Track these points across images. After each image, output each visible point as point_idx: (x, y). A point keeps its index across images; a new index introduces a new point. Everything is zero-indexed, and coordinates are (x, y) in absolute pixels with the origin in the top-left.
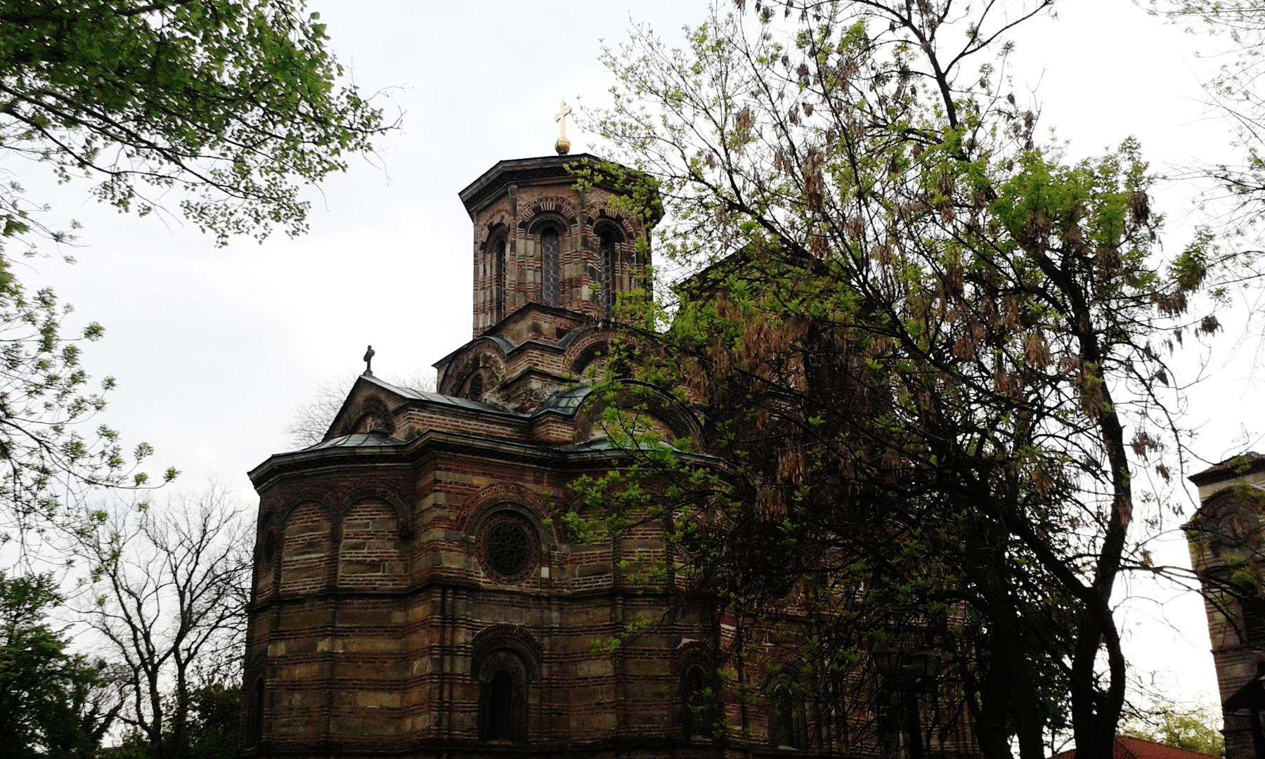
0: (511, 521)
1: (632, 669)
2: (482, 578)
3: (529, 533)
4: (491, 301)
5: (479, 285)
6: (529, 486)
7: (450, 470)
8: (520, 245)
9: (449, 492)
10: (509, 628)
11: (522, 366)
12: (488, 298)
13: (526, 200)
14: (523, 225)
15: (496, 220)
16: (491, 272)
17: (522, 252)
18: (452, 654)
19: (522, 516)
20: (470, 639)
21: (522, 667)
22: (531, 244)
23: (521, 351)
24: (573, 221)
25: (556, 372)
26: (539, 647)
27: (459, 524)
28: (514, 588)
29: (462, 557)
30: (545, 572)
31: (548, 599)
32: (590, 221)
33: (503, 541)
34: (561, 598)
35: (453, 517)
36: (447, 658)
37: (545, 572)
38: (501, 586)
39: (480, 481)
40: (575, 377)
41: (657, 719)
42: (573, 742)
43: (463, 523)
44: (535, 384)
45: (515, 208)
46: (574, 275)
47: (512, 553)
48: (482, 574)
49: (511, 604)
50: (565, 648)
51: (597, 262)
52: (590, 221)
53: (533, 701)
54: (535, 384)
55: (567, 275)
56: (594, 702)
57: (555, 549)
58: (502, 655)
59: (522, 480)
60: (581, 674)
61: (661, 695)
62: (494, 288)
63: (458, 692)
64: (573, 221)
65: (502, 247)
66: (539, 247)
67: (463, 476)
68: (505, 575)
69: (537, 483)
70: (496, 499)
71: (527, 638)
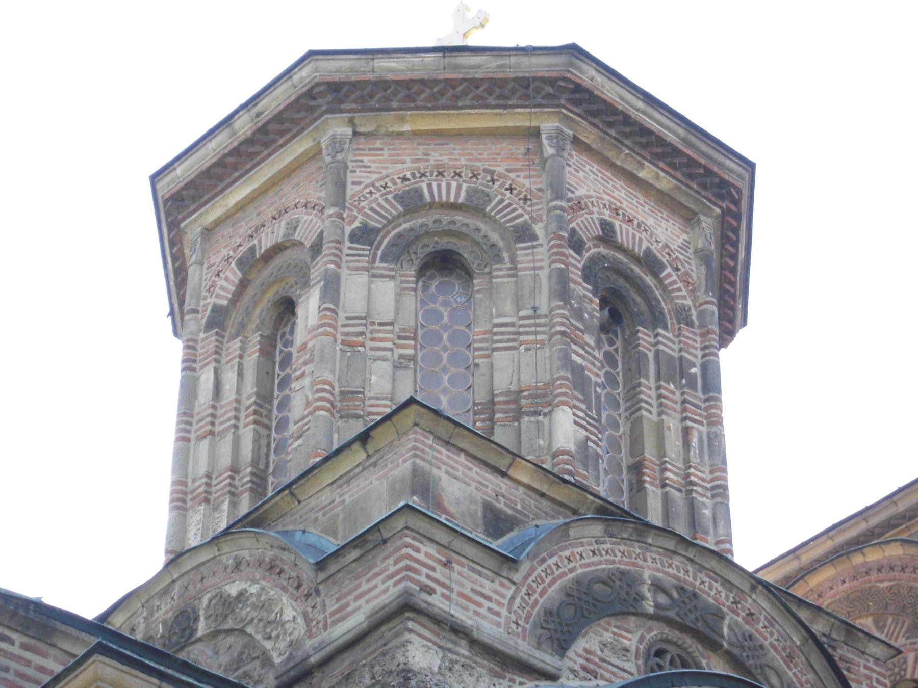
4: (235, 470)
5: (193, 425)
8: (355, 289)
11: (376, 591)
12: (225, 460)
13: (383, 167)
14: (365, 235)
15: (267, 241)
16: (239, 383)
17: (359, 308)
22: (386, 291)
23: (370, 541)
24: (524, 234)
25: (490, 629)
32: (577, 245)
40: (546, 659)
44: (421, 653)
45: (341, 186)
46: (528, 378)
51: (589, 355)
52: (577, 245)
54: (421, 653)
55: (503, 381)
62: (247, 435)
64: (524, 234)
65: (287, 308)
66: (410, 302)
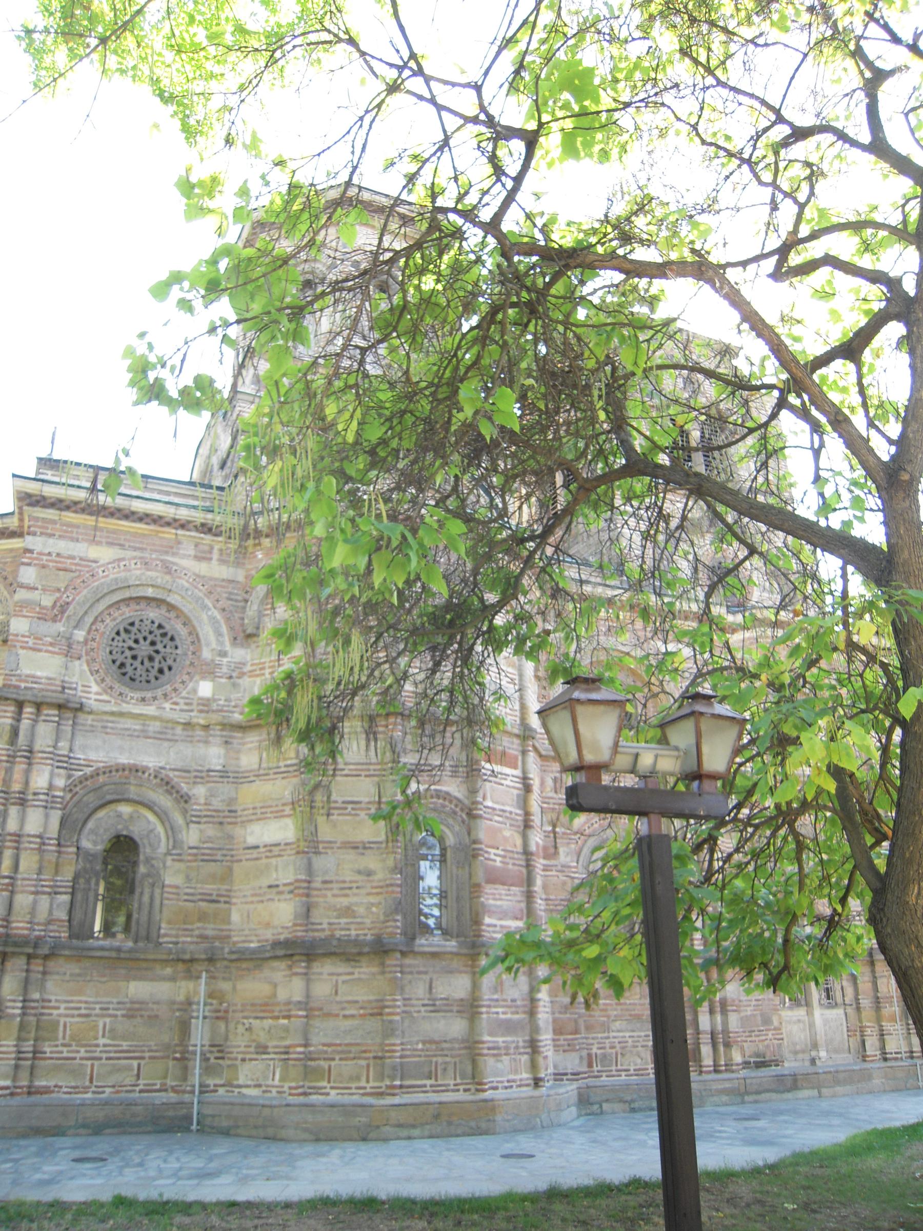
0: (153, 614)
1: (325, 832)
2: (91, 689)
3: (181, 631)
6: (185, 563)
7: (51, 535)
9: (44, 567)
10: (136, 770)
18: (22, 802)
19: (171, 607)
20: (60, 782)
21: (160, 829)
26: (184, 799)
27: (60, 610)
28: (150, 710)
29: (58, 660)
30: (205, 689)
31: (206, 727)
33: (136, 641)
34: (224, 726)
35: (47, 601)
36: (13, 811)
37: (205, 689)
38: (125, 708)
39: (103, 554)
41: (361, 910)
42: (235, 943)
43: (63, 612)
47: (151, 659)
48: (95, 688)
49: (144, 734)
50: (232, 801)
53: (172, 877)
56: (265, 882)
57: (223, 654)
58: (125, 809)
59: (174, 554)
60: (251, 840)
61: (369, 873)
63: (28, 862)
67: (72, 545)
68: (133, 689)
69: (198, 558)
70: (126, 579)
71: (168, 785)
